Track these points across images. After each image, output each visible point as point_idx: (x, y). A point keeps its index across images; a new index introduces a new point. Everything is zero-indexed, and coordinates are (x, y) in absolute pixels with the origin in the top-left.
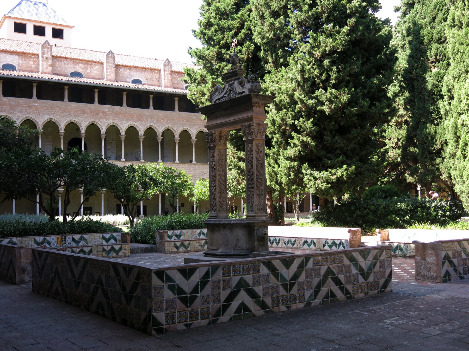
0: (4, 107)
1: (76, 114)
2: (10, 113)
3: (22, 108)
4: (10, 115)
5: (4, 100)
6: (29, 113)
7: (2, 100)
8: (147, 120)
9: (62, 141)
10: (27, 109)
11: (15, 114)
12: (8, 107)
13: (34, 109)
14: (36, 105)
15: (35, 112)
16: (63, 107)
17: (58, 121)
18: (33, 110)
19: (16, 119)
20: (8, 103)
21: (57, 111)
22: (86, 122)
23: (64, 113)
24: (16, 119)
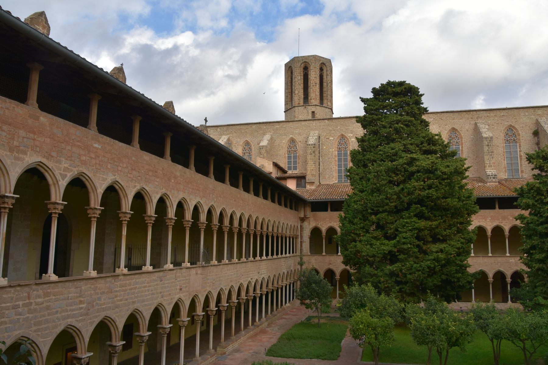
0: (40, 139)
1: (148, 177)
2: (49, 157)
3: (74, 149)
4: (50, 164)
5: (42, 119)
6: (84, 163)
7: (37, 119)
8: (210, 196)
9: (124, 232)
10: (82, 152)
11: (60, 162)
12: (48, 140)
13: (93, 155)
14: (96, 145)
15: (94, 161)
16: (133, 158)
17: (125, 187)
18: (91, 158)
19: (61, 174)
20: (48, 128)
21: (125, 165)
22: (157, 193)
23: (134, 172)
24: (61, 174)
